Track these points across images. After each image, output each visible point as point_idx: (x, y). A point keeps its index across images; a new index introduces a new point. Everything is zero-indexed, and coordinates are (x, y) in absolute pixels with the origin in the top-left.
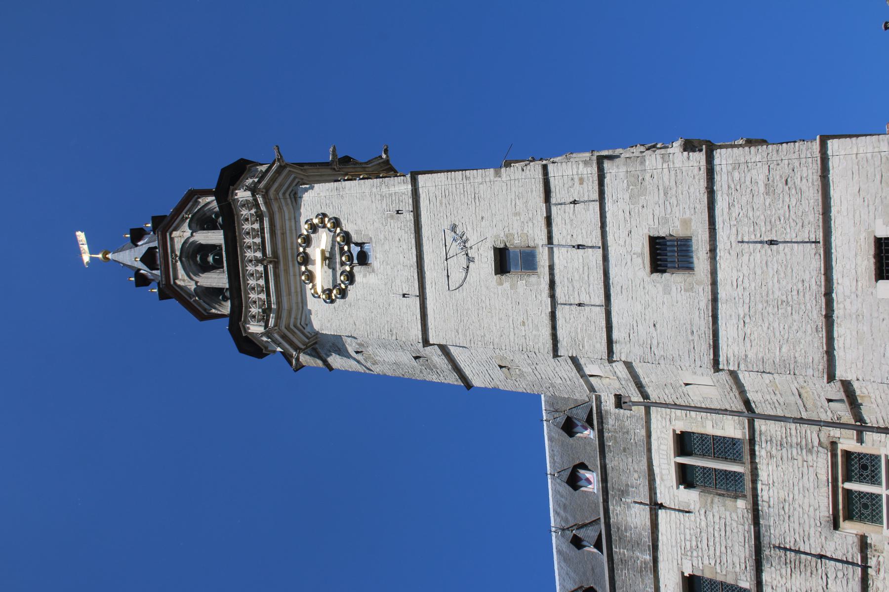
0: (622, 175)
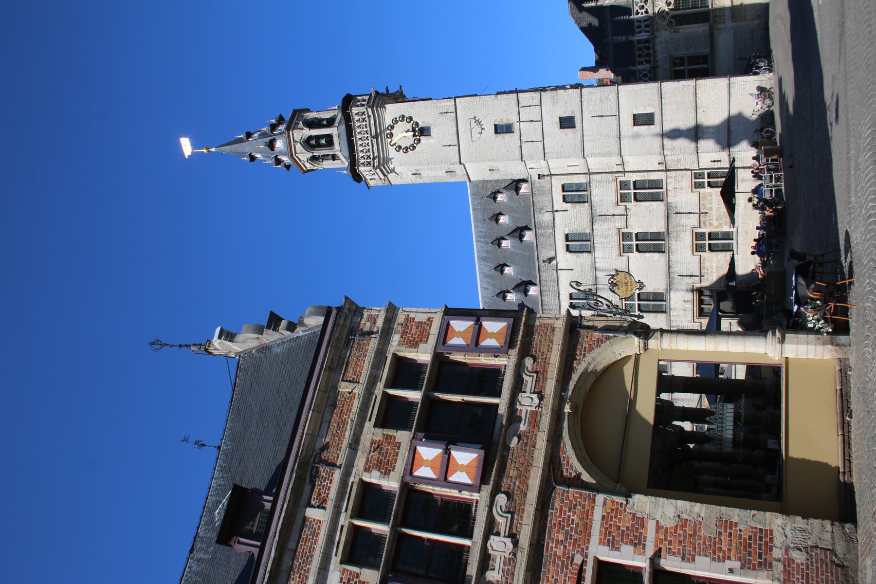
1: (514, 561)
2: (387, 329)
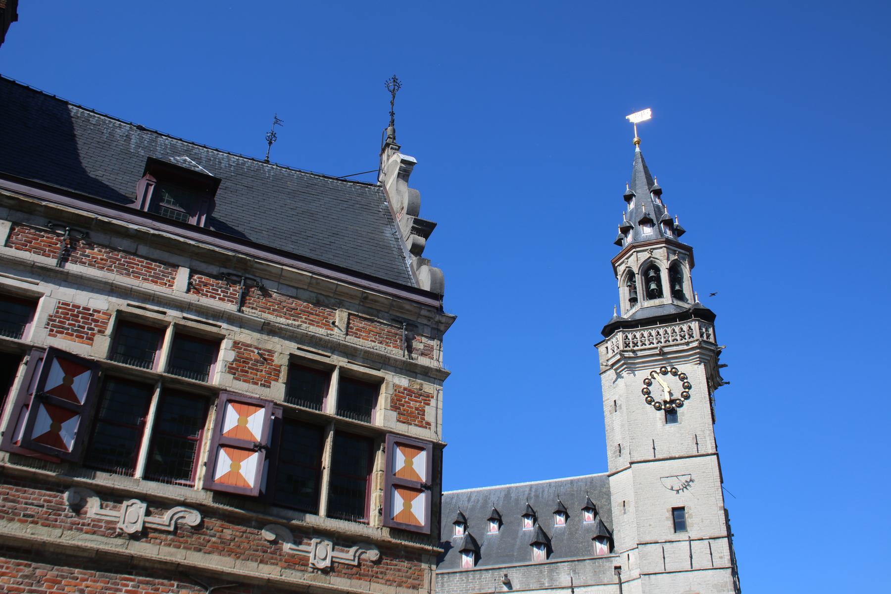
0: (725, 579)
1: (111, 535)
2: (415, 371)
